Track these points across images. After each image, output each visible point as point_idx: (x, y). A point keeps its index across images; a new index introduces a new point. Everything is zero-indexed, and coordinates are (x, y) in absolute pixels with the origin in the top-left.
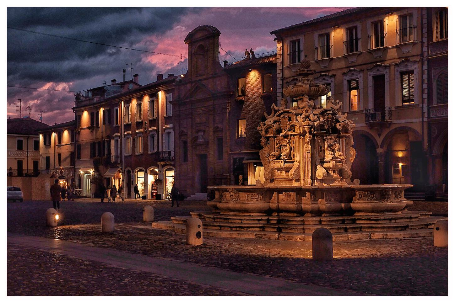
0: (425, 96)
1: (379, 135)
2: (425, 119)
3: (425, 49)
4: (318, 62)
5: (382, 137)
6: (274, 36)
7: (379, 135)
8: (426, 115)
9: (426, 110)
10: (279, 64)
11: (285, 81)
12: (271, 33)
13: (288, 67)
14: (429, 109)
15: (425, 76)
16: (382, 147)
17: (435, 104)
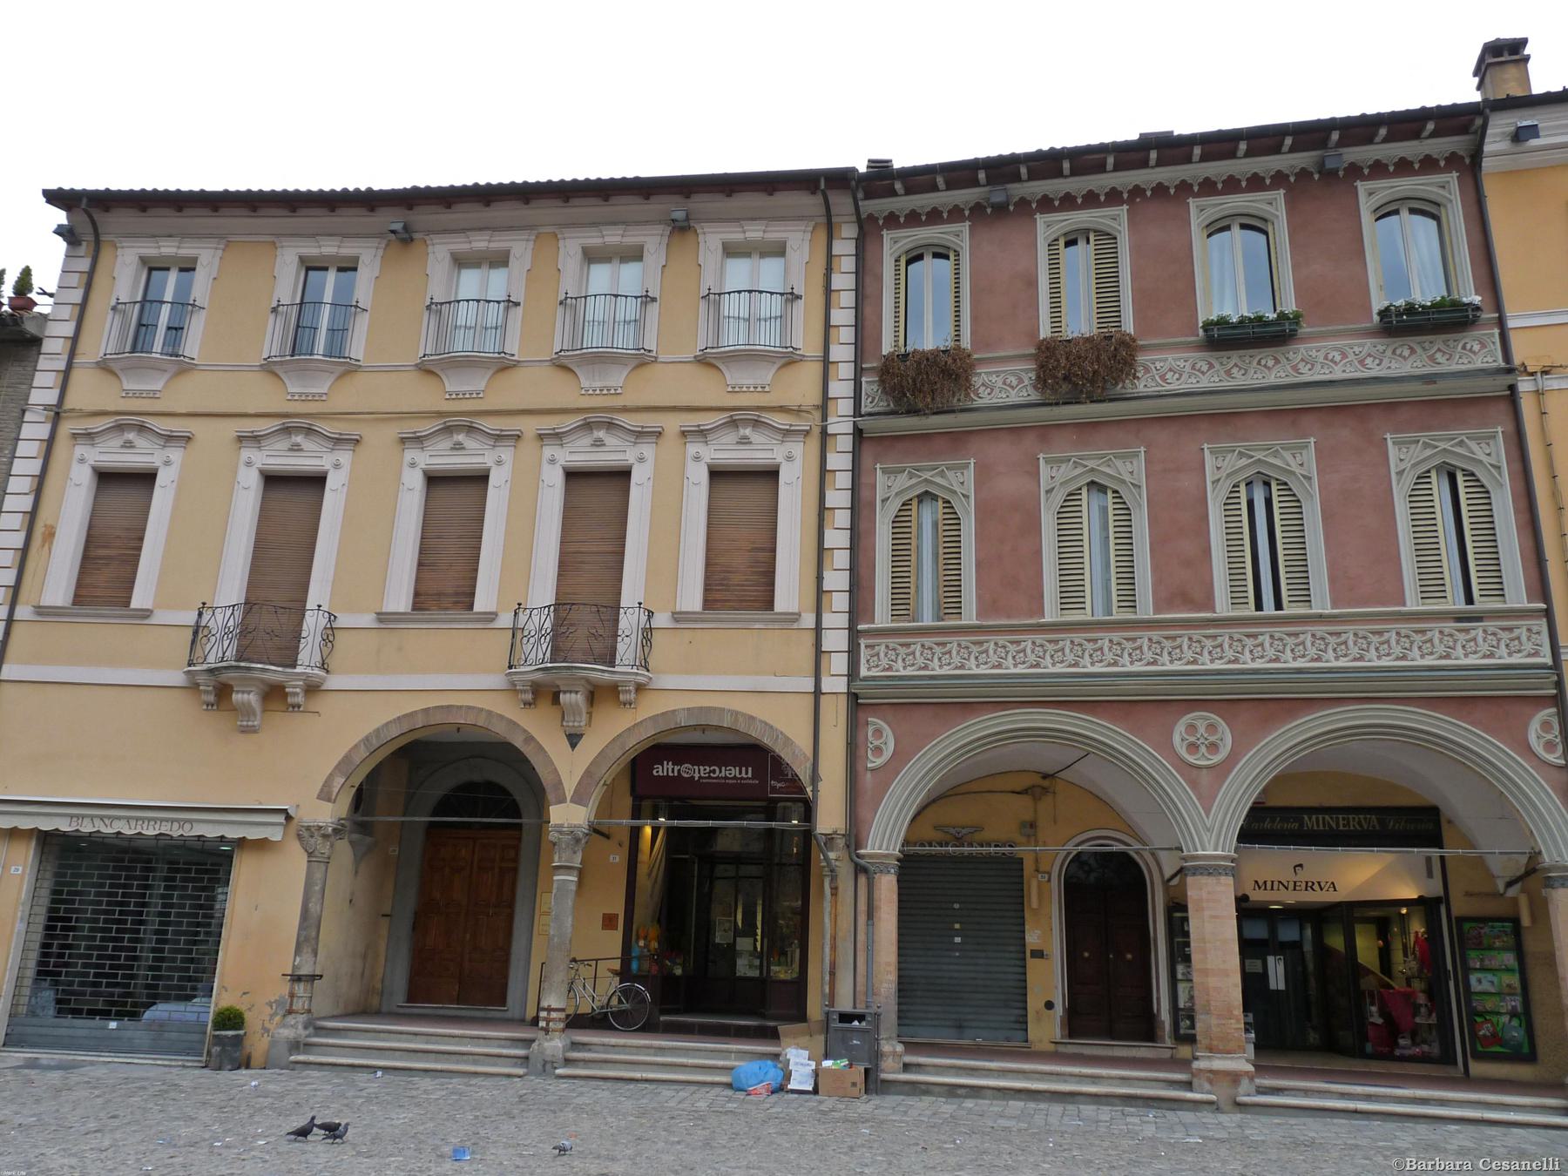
0: (837, 580)
1: (574, 739)
2: (835, 683)
3: (841, 388)
4: (277, 369)
5: (591, 747)
6: (60, 217)
7: (574, 739)
8: (839, 663)
9: (835, 640)
10: (55, 346)
11: (66, 428)
12: (55, 197)
13: (104, 366)
14: (854, 634)
15: (839, 498)
16: (579, 798)
17: (882, 616)
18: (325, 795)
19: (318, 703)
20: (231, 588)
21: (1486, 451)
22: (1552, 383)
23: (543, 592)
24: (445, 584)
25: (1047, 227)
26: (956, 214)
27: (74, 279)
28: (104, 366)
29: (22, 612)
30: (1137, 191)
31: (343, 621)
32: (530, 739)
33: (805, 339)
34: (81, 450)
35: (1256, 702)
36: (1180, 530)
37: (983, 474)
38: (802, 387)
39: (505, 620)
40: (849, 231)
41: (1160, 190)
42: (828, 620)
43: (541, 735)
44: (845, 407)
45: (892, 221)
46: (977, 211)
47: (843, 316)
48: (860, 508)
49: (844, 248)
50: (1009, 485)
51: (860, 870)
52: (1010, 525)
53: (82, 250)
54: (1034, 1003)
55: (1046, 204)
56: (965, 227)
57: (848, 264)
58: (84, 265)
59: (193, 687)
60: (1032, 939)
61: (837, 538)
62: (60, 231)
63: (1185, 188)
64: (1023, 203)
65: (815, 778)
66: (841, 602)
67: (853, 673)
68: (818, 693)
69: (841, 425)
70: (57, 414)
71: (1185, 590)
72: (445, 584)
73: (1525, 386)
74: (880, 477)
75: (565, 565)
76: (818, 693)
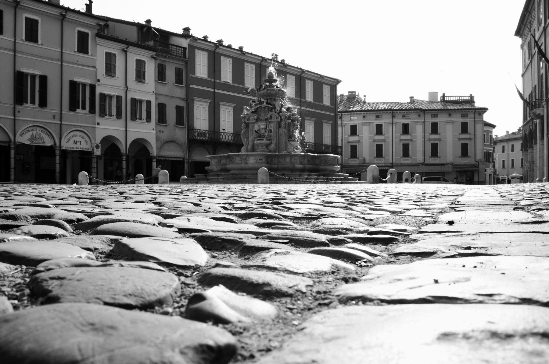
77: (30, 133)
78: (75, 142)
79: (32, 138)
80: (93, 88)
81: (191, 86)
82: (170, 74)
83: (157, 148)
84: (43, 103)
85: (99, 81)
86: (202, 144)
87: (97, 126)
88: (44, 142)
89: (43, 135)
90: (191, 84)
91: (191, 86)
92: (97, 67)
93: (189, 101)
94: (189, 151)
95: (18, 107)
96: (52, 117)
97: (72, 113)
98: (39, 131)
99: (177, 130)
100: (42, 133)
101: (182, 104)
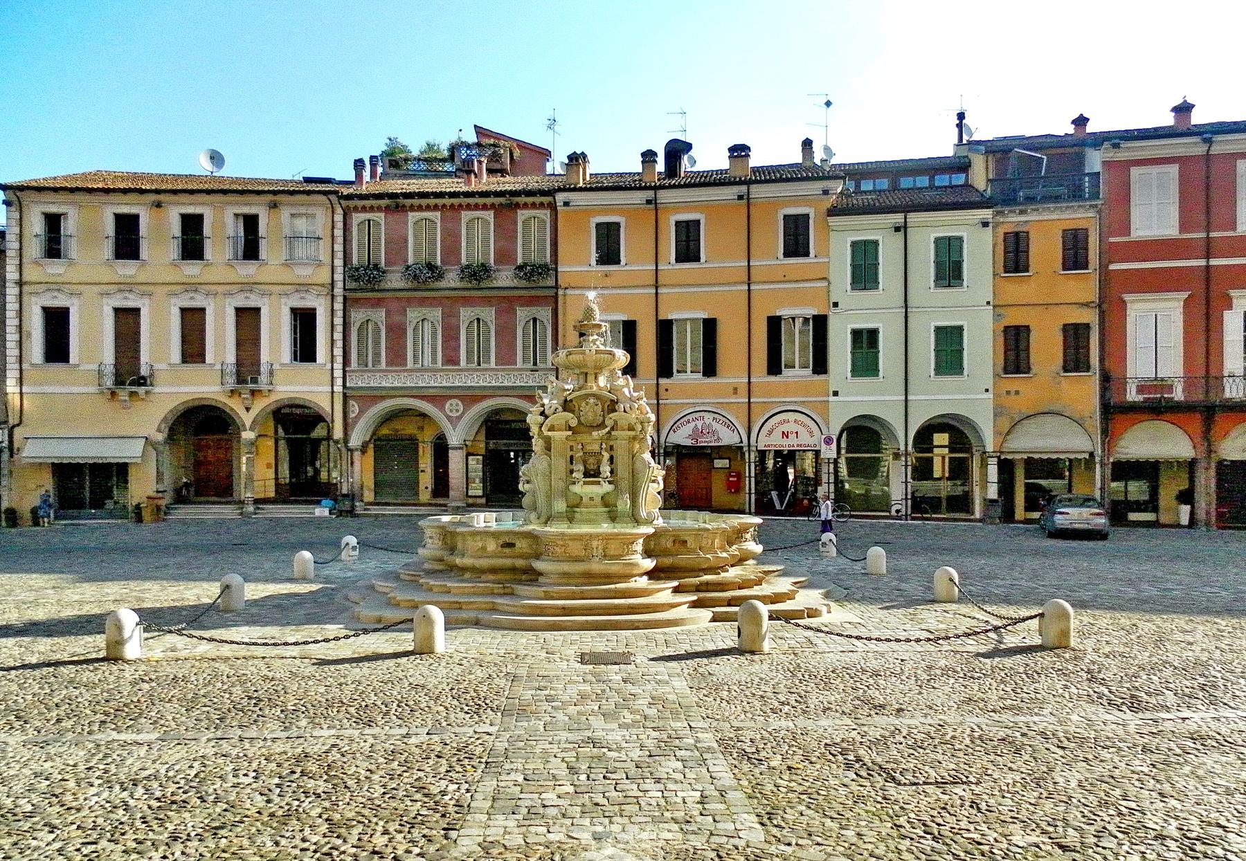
0: (338, 352)
1: (248, 409)
2: (338, 388)
3: (339, 277)
7: (248, 409)
8: (339, 382)
9: (338, 373)
11: (26, 288)
15: (338, 321)
16: (251, 429)
17: (354, 364)
18: (159, 430)
19: (151, 397)
20: (109, 357)
21: (544, 314)
22: (568, 292)
23: (231, 358)
24: (193, 350)
25: (413, 216)
26: (379, 209)
27: (14, 223)
28: (36, 263)
29: (25, 366)
30: (444, 206)
31: (156, 366)
32: (232, 409)
33: (325, 256)
34: (34, 299)
35: (470, 397)
36: (451, 336)
37: (388, 313)
38: (324, 276)
39: (218, 367)
40: (339, 211)
41: (452, 206)
42: (335, 366)
43: (235, 405)
44: (339, 285)
45: (356, 209)
46: (387, 208)
47: (339, 247)
48: (346, 325)
49: (339, 218)
50: (397, 318)
51: (349, 450)
52: (397, 333)
53: (13, 209)
54: (422, 487)
55: (412, 208)
56: (382, 215)
57: (340, 225)
58: (17, 215)
59: (102, 393)
60: (422, 466)
61: (338, 336)
62: (5, 202)
63: (460, 205)
64: (404, 206)
65: (333, 421)
66: (339, 359)
67: (344, 386)
68: (333, 392)
69: (339, 290)
70: (20, 284)
71: (451, 360)
72: (193, 350)
73: (561, 292)
74: (353, 314)
75: (239, 344)
76: (333, 392)
77: (692, 425)
78: (785, 435)
79: (696, 434)
80: (820, 324)
81: (1112, 267)
82: (1046, 250)
83: (997, 433)
84: (710, 368)
85: (836, 305)
86: (1157, 408)
87: (832, 398)
88: (719, 438)
89: (716, 426)
90: (1111, 262)
91: (1112, 267)
92: (831, 279)
93: (1110, 307)
94: (1105, 432)
95: (663, 381)
96: (731, 390)
97: (773, 379)
98: (709, 418)
99: (1065, 384)
100: (714, 423)
101: (1090, 317)
